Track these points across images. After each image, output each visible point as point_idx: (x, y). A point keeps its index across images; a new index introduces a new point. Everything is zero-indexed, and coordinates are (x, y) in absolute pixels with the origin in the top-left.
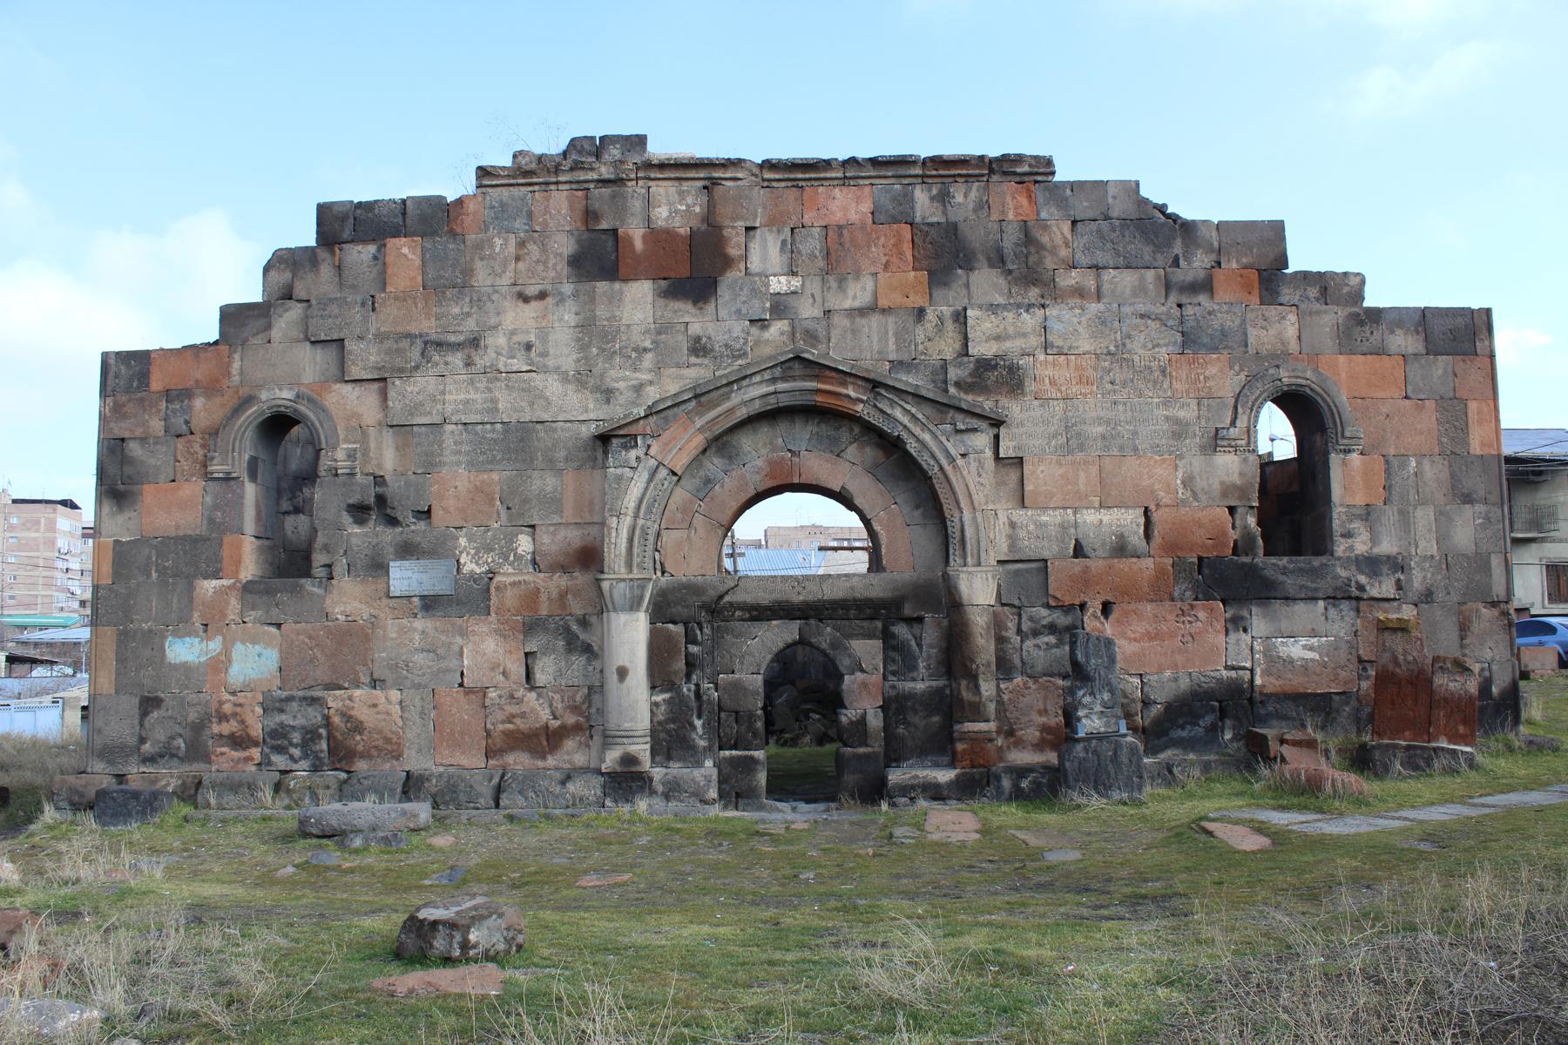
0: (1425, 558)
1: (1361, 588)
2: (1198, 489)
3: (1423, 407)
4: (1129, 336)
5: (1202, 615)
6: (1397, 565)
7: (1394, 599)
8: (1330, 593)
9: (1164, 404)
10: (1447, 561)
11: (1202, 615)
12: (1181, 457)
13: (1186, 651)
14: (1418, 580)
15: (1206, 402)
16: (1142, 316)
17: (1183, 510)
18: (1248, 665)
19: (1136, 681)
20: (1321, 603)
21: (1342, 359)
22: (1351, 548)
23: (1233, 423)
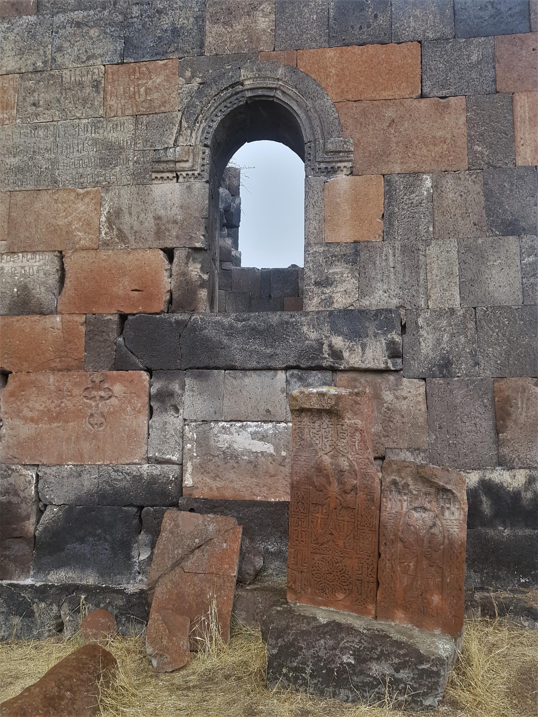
0: (440, 313)
1: (337, 355)
2: (126, 229)
3: (447, 106)
4: (60, 49)
5: (118, 388)
6: (396, 322)
7: (387, 371)
8: (292, 362)
9: (94, 125)
10: (479, 315)
11: (118, 388)
12: (107, 189)
13: (95, 437)
14: (428, 344)
15: (145, 119)
16: (78, 25)
17: (103, 254)
18: (175, 458)
19: (31, 474)
20: (281, 376)
21: (330, 53)
22: (330, 301)
23: (175, 145)
